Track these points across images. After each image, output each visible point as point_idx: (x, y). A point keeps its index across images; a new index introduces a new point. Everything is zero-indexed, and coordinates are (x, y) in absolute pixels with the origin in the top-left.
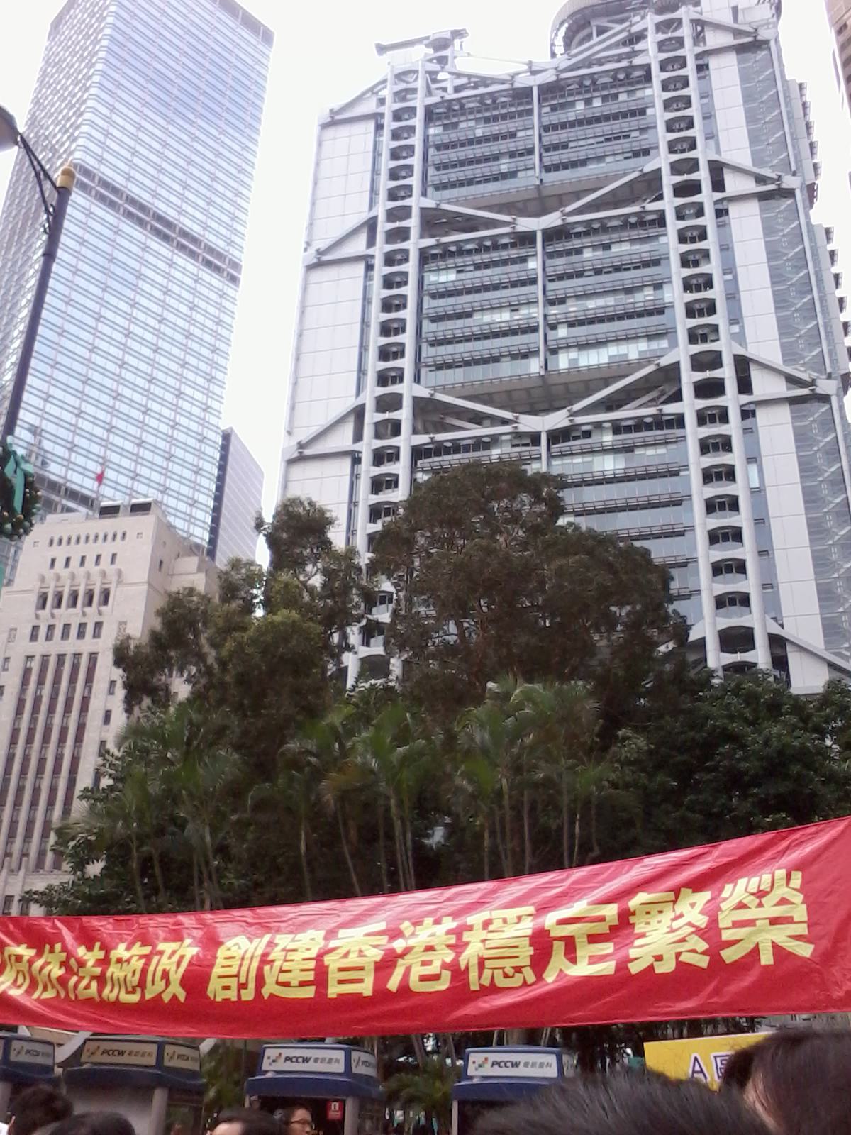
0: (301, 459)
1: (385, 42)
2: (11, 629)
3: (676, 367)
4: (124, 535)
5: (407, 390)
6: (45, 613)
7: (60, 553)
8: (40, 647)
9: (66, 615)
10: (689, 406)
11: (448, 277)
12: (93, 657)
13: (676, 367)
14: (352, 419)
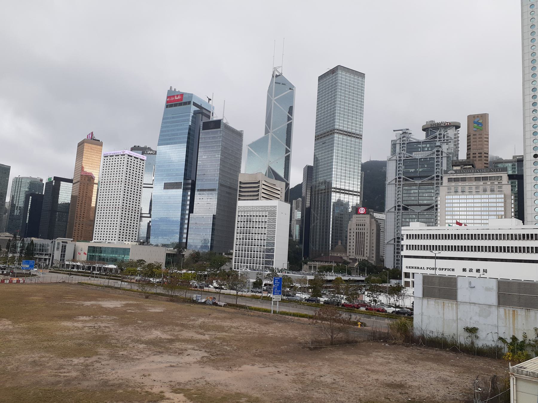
1: (394, 129)
7: (358, 219)
8: (357, 231)
9: (360, 227)
11: (406, 188)
12: (364, 233)
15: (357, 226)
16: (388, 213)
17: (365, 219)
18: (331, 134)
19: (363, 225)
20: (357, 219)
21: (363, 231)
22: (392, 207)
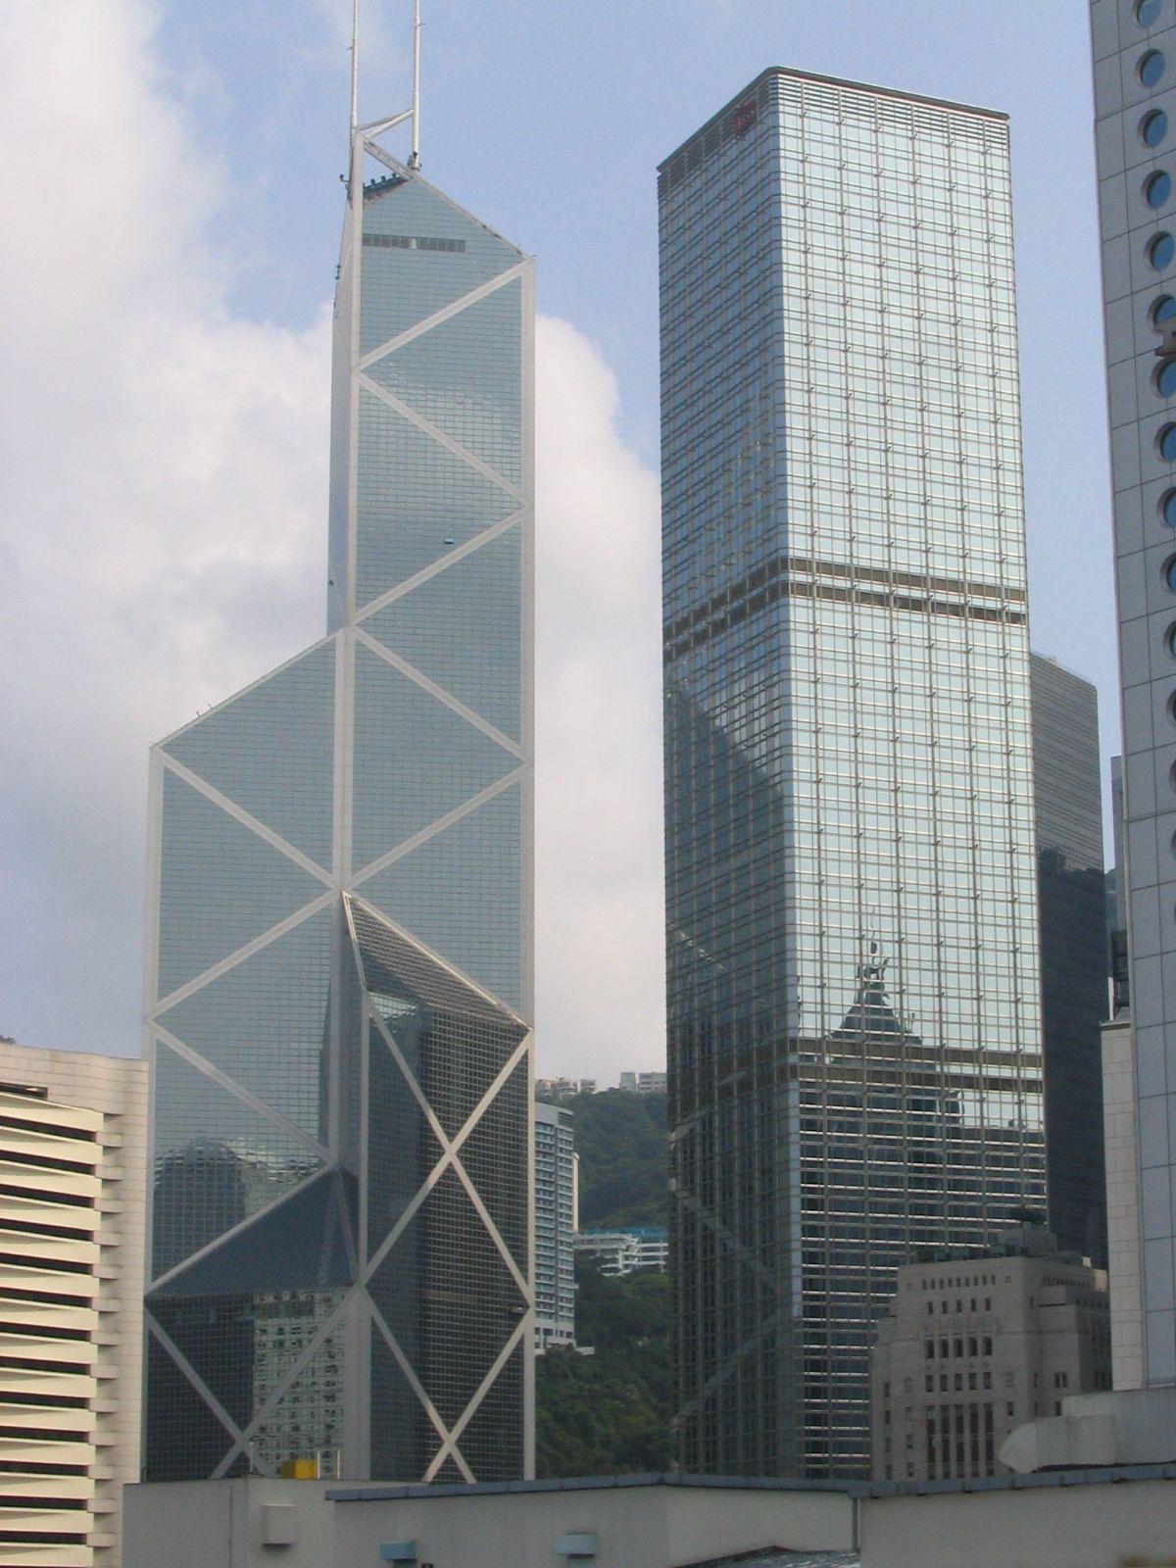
4: (993, 1278)
7: (935, 1297)
8: (937, 1398)
9: (954, 1365)
12: (988, 1407)
15: (930, 1354)
17: (987, 1291)
18: (758, 603)
21: (980, 1397)
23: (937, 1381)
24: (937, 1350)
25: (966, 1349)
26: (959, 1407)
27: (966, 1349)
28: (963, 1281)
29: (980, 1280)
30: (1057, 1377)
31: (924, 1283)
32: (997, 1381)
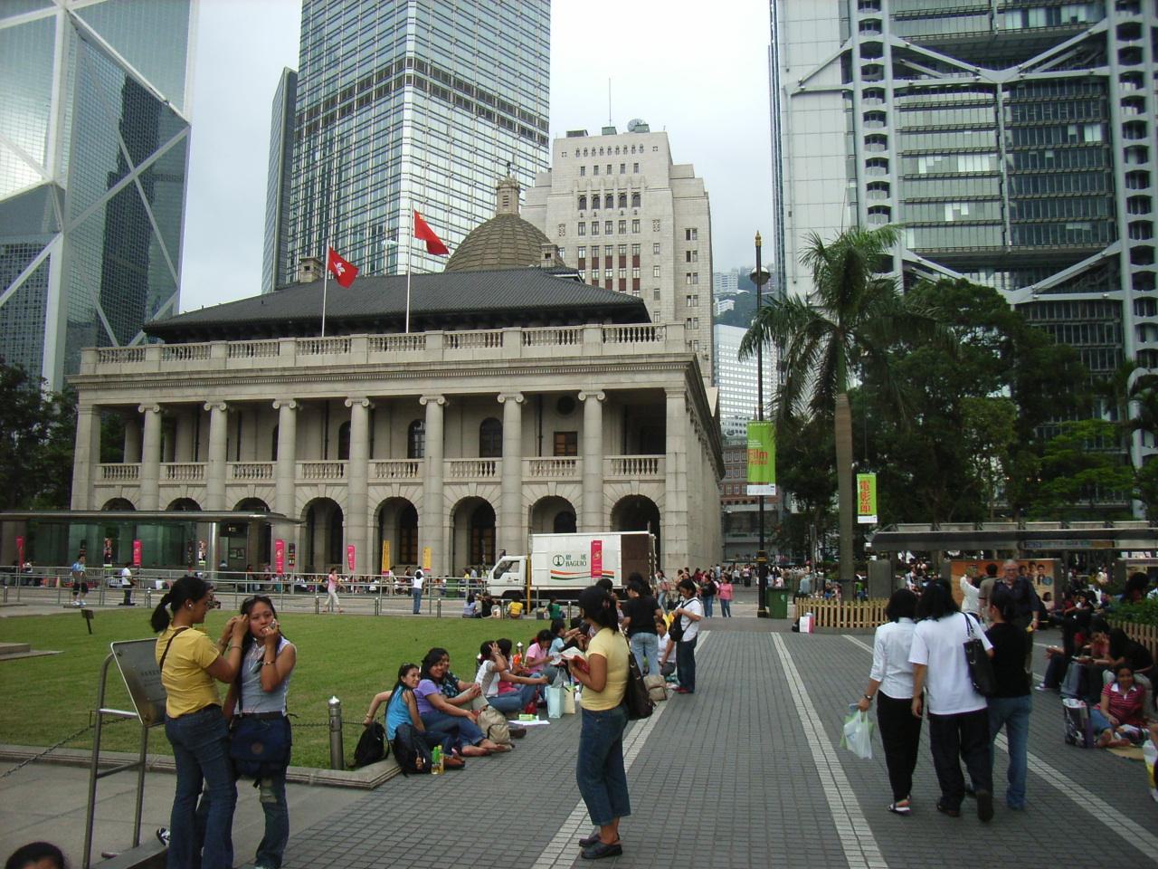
0: (803, 93)
2: (560, 226)
3: (1103, 37)
4: (642, 147)
5: (889, 38)
6: (589, 211)
7: (589, 162)
8: (588, 240)
9: (604, 213)
10: (1114, 69)
13: (1103, 37)
14: (839, 60)
16: (799, 103)
17: (637, 157)
19: (623, 197)
20: (583, 161)
21: (629, 238)
22: (823, 61)
23: (589, 226)
24: (589, 202)
25: (616, 201)
26: (609, 247)
27: (616, 201)
28: (613, 149)
29: (629, 149)
30: (688, 232)
31: (578, 151)
32: (645, 226)
